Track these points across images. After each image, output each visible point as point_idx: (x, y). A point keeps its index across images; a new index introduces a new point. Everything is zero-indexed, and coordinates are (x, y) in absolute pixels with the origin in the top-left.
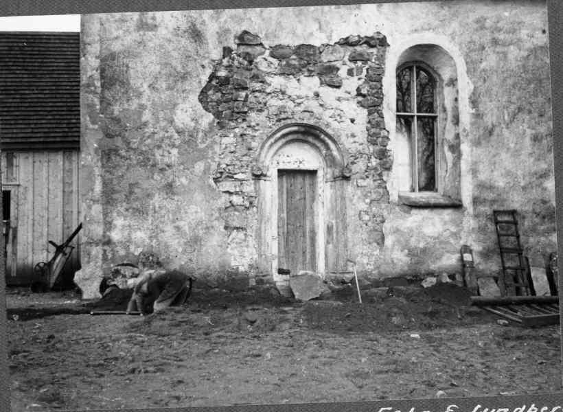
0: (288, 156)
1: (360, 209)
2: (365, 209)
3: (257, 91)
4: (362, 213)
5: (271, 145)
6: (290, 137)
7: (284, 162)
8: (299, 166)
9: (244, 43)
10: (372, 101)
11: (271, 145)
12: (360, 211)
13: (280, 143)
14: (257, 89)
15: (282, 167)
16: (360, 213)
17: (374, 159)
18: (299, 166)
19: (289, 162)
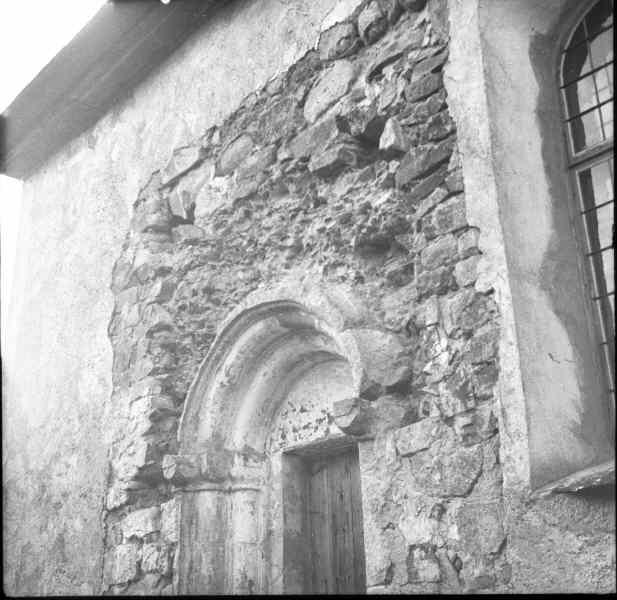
0: (303, 410)
1: (412, 539)
2: (427, 538)
3: (189, 268)
4: (417, 553)
5: (233, 388)
6: (279, 357)
7: (295, 430)
8: (328, 431)
9: (176, 174)
10: (422, 157)
11: (233, 388)
12: (412, 548)
13: (259, 381)
14: (187, 262)
15: (292, 442)
16: (410, 560)
17: (444, 342)
18: (328, 431)
19: (305, 427)
